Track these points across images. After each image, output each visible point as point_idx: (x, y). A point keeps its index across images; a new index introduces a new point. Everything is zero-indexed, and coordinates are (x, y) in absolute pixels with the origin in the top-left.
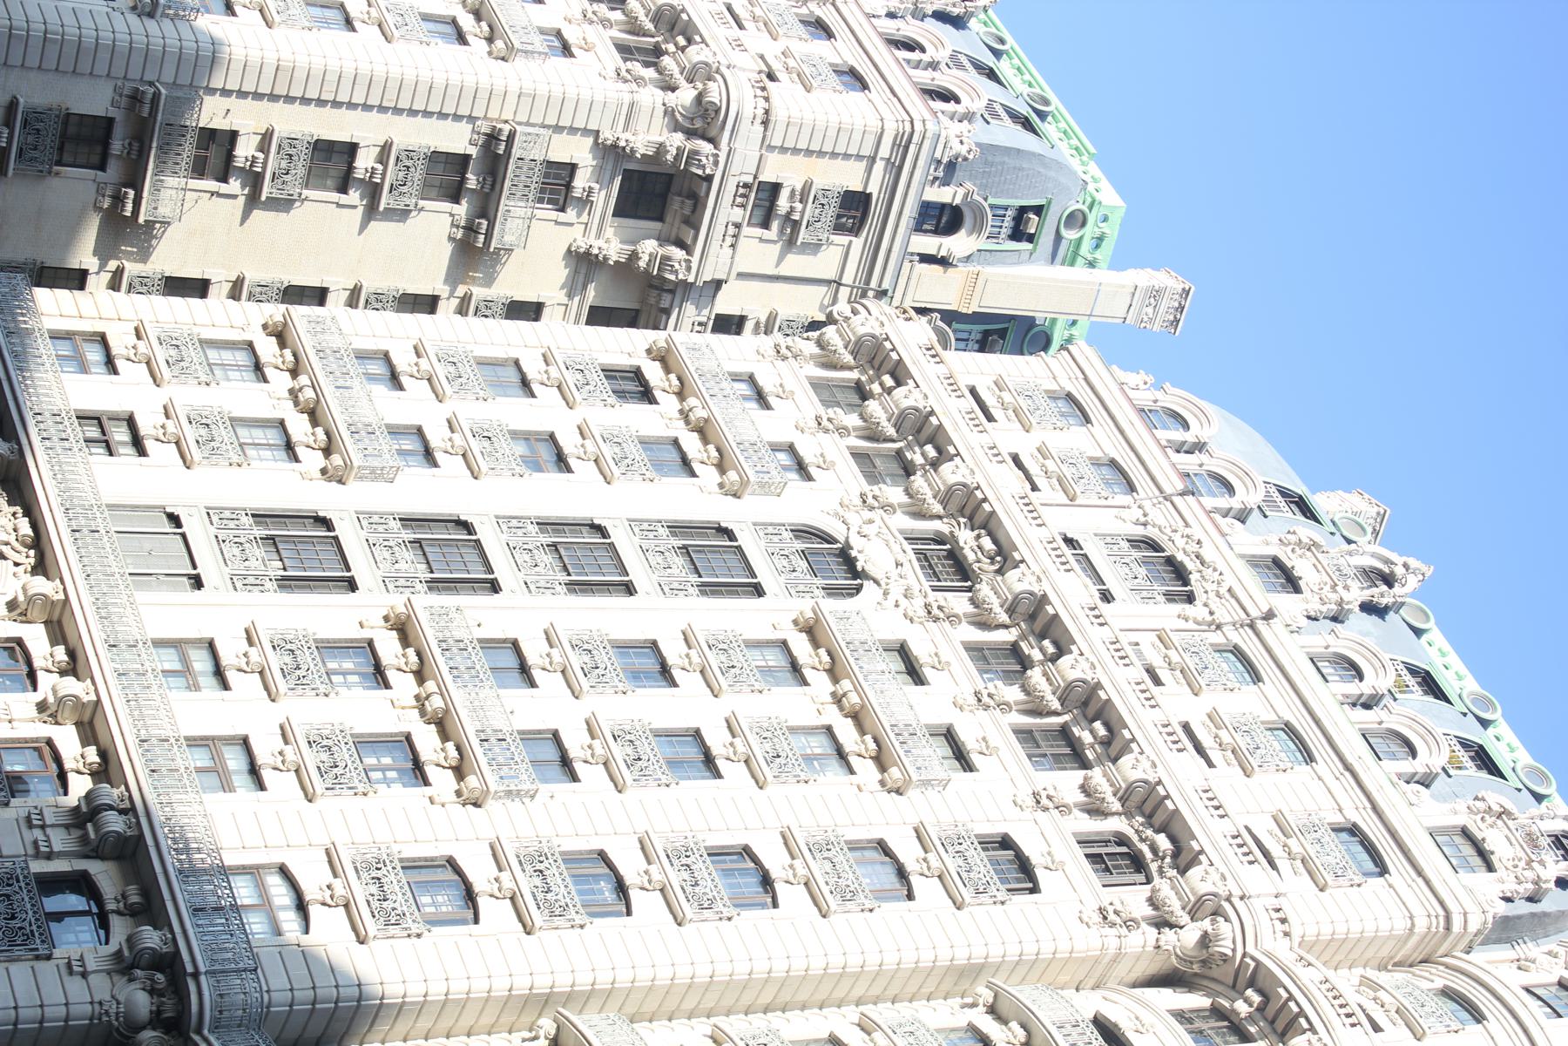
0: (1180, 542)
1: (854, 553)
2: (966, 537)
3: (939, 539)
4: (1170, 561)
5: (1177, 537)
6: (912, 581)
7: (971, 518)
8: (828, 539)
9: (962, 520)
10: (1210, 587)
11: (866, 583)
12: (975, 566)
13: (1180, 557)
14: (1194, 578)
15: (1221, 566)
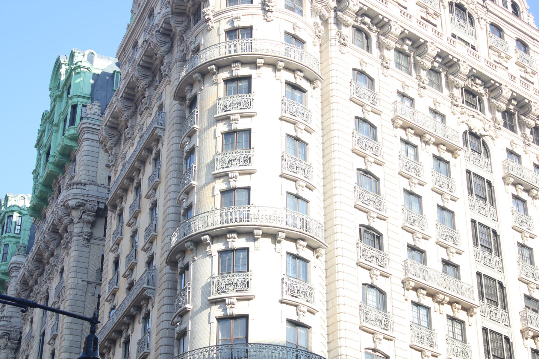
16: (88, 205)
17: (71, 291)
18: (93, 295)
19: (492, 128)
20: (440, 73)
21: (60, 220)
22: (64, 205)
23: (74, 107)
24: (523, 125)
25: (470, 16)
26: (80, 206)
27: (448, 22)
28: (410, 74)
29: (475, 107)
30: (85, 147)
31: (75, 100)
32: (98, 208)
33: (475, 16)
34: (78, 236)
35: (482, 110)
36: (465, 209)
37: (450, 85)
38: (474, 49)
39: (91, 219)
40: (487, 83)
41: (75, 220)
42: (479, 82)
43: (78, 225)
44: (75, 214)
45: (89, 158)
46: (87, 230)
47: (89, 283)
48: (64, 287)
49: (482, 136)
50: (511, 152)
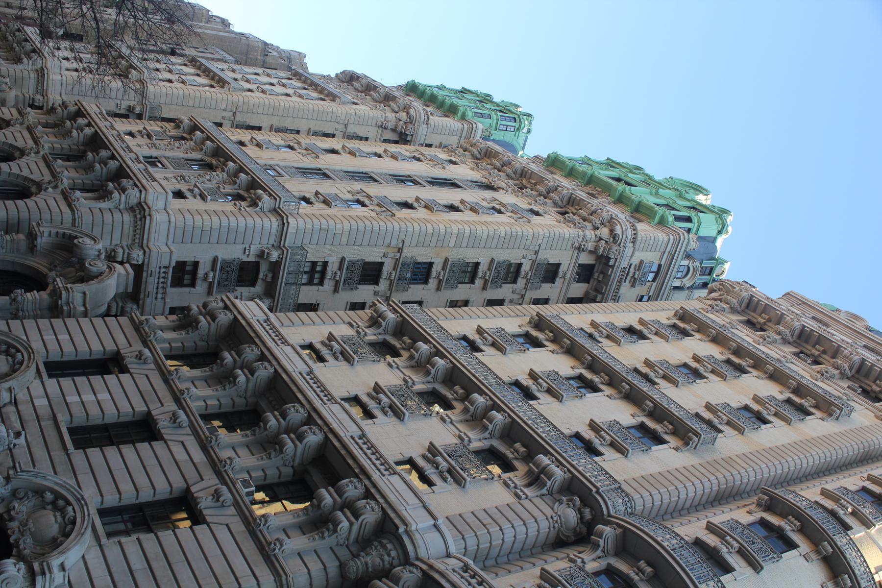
16: (615, 248)
17: (531, 234)
18: (524, 257)
21: (595, 212)
22: (612, 218)
23: (689, 219)
26: (614, 238)
30: (661, 236)
31: (695, 219)
32: (610, 259)
34: (584, 236)
39: (601, 251)
41: (598, 232)
43: (593, 236)
44: (604, 232)
45: (651, 243)
46: (590, 246)
47: (536, 253)
48: (529, 221)
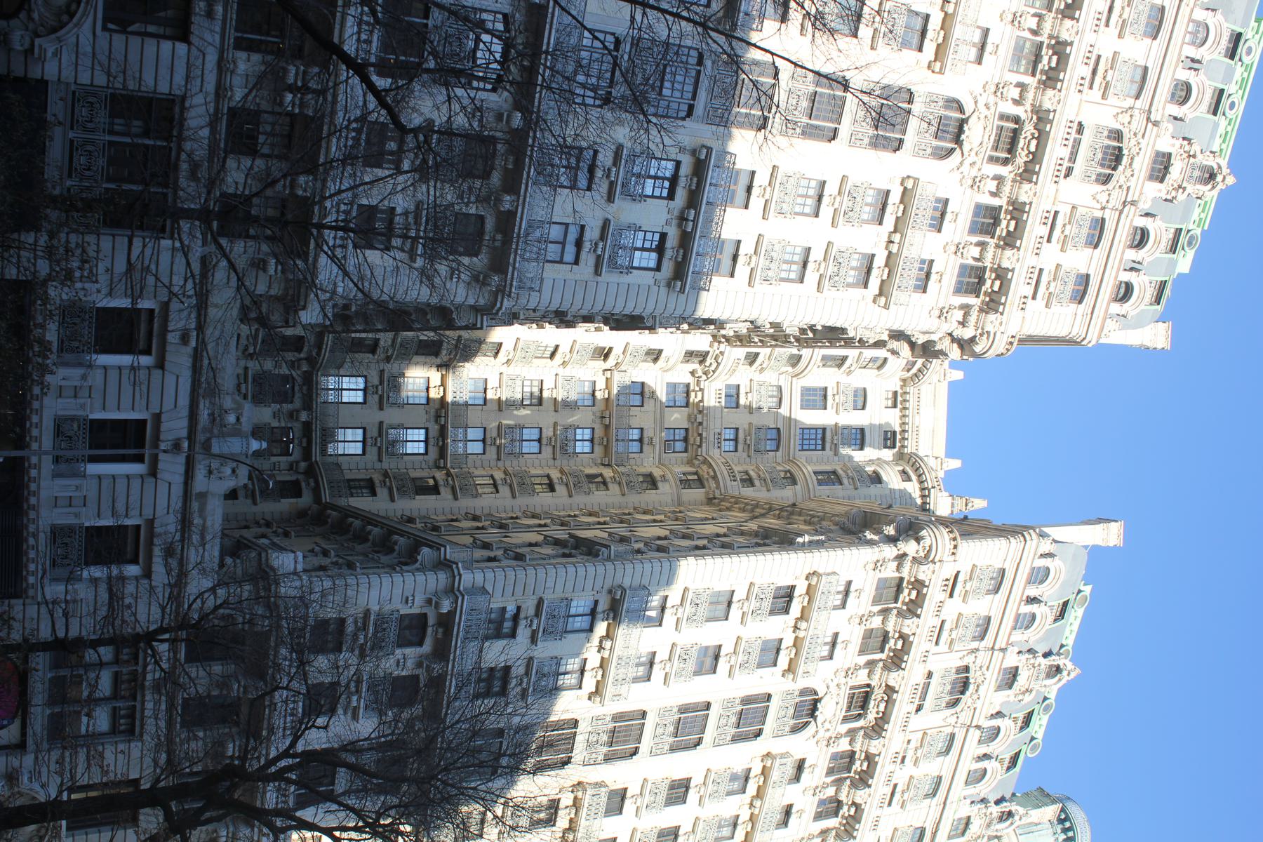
0: (1133, 142)
1: (966, 127)
2: (1029, 129)
3: (1017, 120)
4: (1120, 149)
5: (1133, 142)
6: (978, 160)
7: (1039, 119)
8: (961, 110)
9: (1035, 117)
10: (1122, 180)
11: (958, 150)
12: (1019, 150)
13: (1125, 152)
14: (1121, 168)
15: (1136, 173)
19: (828, 735)
20: (882, 651)
24: (838, 783)
25: (957, 702)
27: (945, 662)
28: (876, 601)
29: (849, 708)
33: (958, 708)
35: (846, 720)
36: (723, 690)
37: (871, 664)
38: (918, 710)
40: (884, 719)
42: (882, 708)
49: (815, 718)
50: (800, 766)
